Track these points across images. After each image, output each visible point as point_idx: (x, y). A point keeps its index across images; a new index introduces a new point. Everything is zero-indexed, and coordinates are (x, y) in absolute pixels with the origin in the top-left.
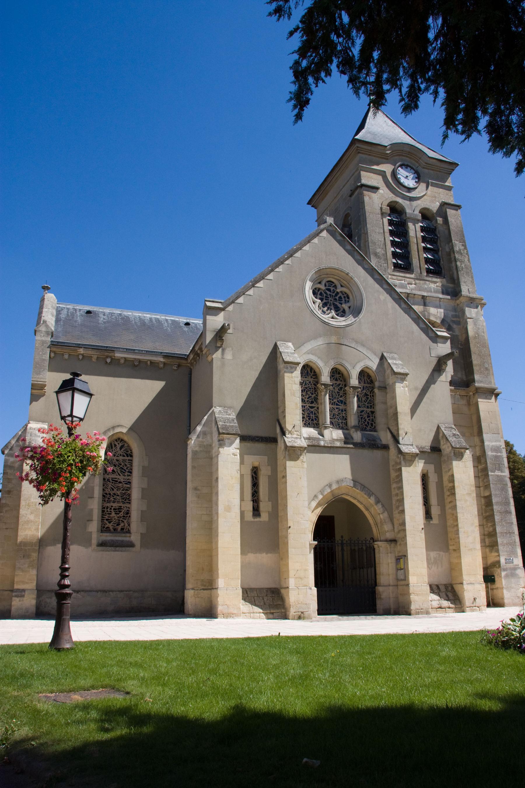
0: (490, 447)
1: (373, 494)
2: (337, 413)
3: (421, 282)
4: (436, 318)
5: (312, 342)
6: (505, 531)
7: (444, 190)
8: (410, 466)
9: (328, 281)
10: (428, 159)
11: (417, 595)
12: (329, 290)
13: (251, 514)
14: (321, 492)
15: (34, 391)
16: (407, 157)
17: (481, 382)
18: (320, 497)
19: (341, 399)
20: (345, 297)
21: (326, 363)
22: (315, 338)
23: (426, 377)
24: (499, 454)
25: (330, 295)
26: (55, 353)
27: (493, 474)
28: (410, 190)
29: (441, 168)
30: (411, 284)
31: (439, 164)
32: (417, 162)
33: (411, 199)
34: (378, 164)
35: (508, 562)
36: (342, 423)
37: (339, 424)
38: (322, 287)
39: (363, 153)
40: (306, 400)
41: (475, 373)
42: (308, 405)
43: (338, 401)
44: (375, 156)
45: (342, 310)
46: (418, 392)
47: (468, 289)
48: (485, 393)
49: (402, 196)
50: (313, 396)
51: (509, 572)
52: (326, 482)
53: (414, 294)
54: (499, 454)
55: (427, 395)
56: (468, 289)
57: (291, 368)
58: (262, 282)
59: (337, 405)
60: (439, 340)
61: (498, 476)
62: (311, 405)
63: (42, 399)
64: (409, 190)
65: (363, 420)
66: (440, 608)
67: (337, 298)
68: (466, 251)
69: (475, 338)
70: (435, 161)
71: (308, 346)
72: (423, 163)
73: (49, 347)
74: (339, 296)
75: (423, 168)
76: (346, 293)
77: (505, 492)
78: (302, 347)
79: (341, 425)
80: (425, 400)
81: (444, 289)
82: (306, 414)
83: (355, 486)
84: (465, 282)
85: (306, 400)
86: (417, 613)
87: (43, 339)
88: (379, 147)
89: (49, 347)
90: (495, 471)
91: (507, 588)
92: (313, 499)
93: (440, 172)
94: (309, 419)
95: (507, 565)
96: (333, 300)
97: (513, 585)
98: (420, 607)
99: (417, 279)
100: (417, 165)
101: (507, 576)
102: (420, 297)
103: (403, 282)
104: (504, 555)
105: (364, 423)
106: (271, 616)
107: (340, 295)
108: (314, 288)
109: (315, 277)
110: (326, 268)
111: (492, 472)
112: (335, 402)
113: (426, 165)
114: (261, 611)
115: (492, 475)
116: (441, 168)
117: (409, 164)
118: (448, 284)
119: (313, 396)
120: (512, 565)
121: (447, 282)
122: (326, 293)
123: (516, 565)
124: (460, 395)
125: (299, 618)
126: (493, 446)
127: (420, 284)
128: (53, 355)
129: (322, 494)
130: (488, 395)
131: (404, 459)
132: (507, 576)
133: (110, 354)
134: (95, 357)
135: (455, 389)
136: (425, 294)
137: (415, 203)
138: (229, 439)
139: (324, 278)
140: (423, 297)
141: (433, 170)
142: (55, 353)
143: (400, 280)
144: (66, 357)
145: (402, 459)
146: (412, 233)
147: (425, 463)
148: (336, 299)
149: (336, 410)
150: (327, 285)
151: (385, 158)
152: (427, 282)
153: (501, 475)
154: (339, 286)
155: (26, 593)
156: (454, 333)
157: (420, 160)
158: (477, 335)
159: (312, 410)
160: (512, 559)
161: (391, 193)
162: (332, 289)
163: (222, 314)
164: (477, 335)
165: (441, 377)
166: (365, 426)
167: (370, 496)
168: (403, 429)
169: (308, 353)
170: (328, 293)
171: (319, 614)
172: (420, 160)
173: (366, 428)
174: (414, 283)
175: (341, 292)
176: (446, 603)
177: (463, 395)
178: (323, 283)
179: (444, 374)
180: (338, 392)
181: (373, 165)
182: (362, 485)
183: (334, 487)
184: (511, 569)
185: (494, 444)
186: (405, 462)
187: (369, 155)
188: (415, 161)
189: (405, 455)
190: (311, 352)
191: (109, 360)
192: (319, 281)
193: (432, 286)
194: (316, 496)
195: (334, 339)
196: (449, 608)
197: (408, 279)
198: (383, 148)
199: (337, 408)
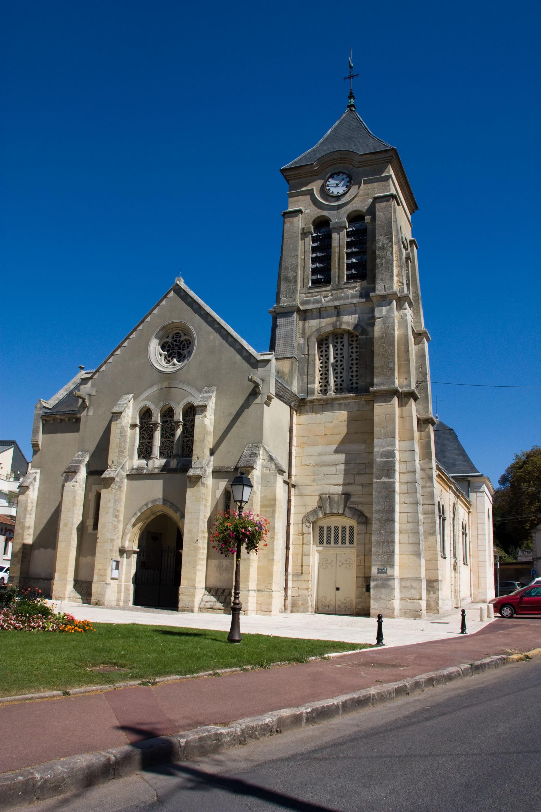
0: (380, 452)
1: (179, 510)
2: (167, 445)
3: (338, 291)
4: (349, 325)
5: (148, 390)
6: (383, 540)
7: (379, 183)
8: (193, 487)
9: (176, 334)
10: (360, 157)
11: (186, 595)
12: (176, 341)
13: (92, 528)
14: (140, 510)
15: (35, 448)
16: (341, 163)
17: (381, 384)
18: (139, 514)
19: (172, 432)
20: (187, 344)
21: (156, 405)
22: (151, 386)
23: (241, 402)
24: (391, 459)
25: (176, 345)
26: (46, 420)
27: (378, 481)
28: (340, 198)
29: (377, 160)
30: (327, 297)
31: (373, 157)
32: (351, 164)
33: (339, 207)
34: (306, 185)
35: (380, 572)
36: (171, 452)
37: (168, 454)
38: (169, 340)
39: (292, 180)
40: (146, 437)
41: (375, 376)
42: (147, 441)
43: (170, 435)
44: (304, 177)
45: (183, 356)
46: (231, 418)
47: (385, 286)
48: (385, 396)
49: (329, 207)
50: (151, 433)
51: (379, 582)
52: (144, 503)
53: (326, 307)
54: (391, 459)
55: (241, 419)
56: (385, 286)
57: (117, 416)
58: (119, 350)
59: (169, 438)
60: (260, 364)
61: (384, 483)
62: (149, 441)
63: (39, 453)
64: (338, 197)
65: (188, 448)
66: (212, 608)
67: (181, 346)
68: (390, 243)
69: (382, 337)
70: (368, 156)
71: (146, 394)
72: (355, 163)
73: (41, 418)
74: (183, 344)
75: (358, 167)
76: (189, 340)
77: (390, 499)
78: (141, 396)
79: (170, 454)
80: (237, 423)
81: (364, 292)
82: (145, 449)
83: (164, 504)
84: (381, 280)
85: (146, 437)
86: (183, 611)
87: (38, 412)
88: (306, 167)
89: (41, 418)
90: (382, 478)
91: (375, 599)
92: (133, 516)
93: (377, 164)
94: (146, 452)
95: (379, 575)
96: (177, 349)
97: (383, 596)
98: (186, 605)
99: (334, 290)
100: (351, 166)
101: (376, 586)
102: (333, 308)
103: (319, 297)
104: (376, 565)
105: (189, 450)
106: (86, 601)
107: (184, 342)
108: (162, 343)
109: (161, 333)
110: (168, 324)
111: (377, 478)
112: (167, 436)
113: (359, 164)
114: (80, 597)
115: (376, 482)
116: (377, 160)
117: (340, 170)
118: (370, 285)
119: (151, 433)
120: (385, 575)
121: (368, 284)
122: (173, 344)
123: (390, 576)
124: (366, 401)
125: (96, 604)
126: (383, 451)
127: (336, 293)
128: (44, 422)
129: (140, 512)
130: (387, 398)
131: (190, 481)
132: (376, 586)
133: (75, 416)
134: (67, 419)
135: (356, 396)
136: (337, 303)
137: (343, 210)
138: (71, 475)
139: (171, 332)
140: (336, 307)
141: (368, 166)
142: (46, 420)
143: (315, 296)
144: (51, 422)
145: (188, 481)
146: (335, 243)
147: (228, 482)
148: (180, 348)
149: (168, 442)
150: (175, 337)
151: (313, 176)
152: (345, 290)
153: (388, 482)
154: (182, 335)
155: (15, 579)
156: (368, 337)
157: (353, 161)
158: (384, 335)
159: (149, 445)
160: (385, 569)
161: (317, 209)
162: (178, 339)
163: (90, 382)
164: (384, 335)
165: (257, 400)
166: (189, 453)
167: (176, 512)
168: (197, 454)
169: (144, 400)
170: (175, 343)
171: (136, 603)
172: (353, 161)
173: (189, 455)
174: (330, 294)
175: (185, 340)
176: (219, 605)
177: (369, 401)
178: (170, 337)
179: (260, 396)
180: (171, 427)
181: (302, 188)
182: (171, 503)
183: (150, 505)
184: (382, 579)
185: (385, 449)
186: (190, 484)
187: (300, 178)
188: (349, 164)
189: (191, 478)
190: (147, 399)
191: (74, 420)
192: (167, 336)
193: (351, 292)
194: (135, 514)
195: (165, 384)
196: (220, 609)
197: (324, 293)
198: (310, 167)
199: (168, 441)
